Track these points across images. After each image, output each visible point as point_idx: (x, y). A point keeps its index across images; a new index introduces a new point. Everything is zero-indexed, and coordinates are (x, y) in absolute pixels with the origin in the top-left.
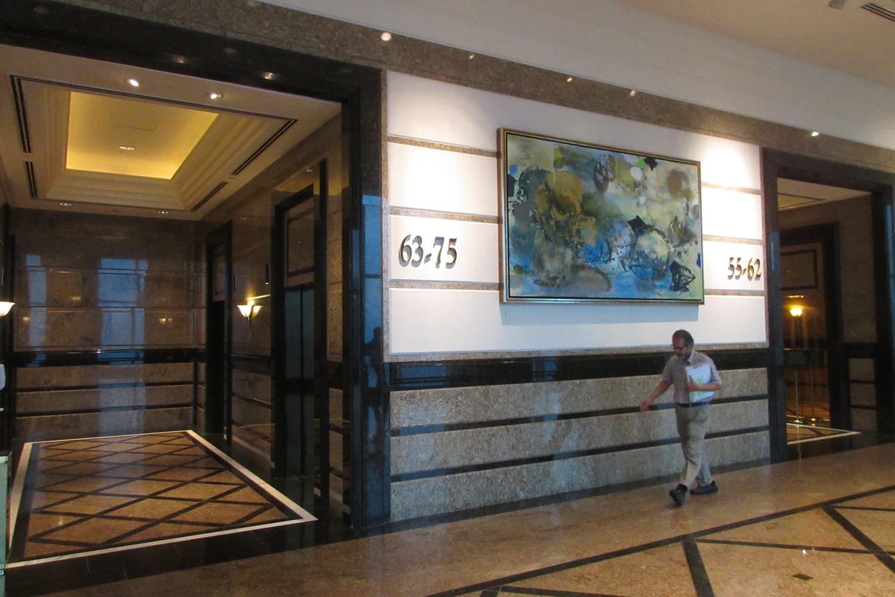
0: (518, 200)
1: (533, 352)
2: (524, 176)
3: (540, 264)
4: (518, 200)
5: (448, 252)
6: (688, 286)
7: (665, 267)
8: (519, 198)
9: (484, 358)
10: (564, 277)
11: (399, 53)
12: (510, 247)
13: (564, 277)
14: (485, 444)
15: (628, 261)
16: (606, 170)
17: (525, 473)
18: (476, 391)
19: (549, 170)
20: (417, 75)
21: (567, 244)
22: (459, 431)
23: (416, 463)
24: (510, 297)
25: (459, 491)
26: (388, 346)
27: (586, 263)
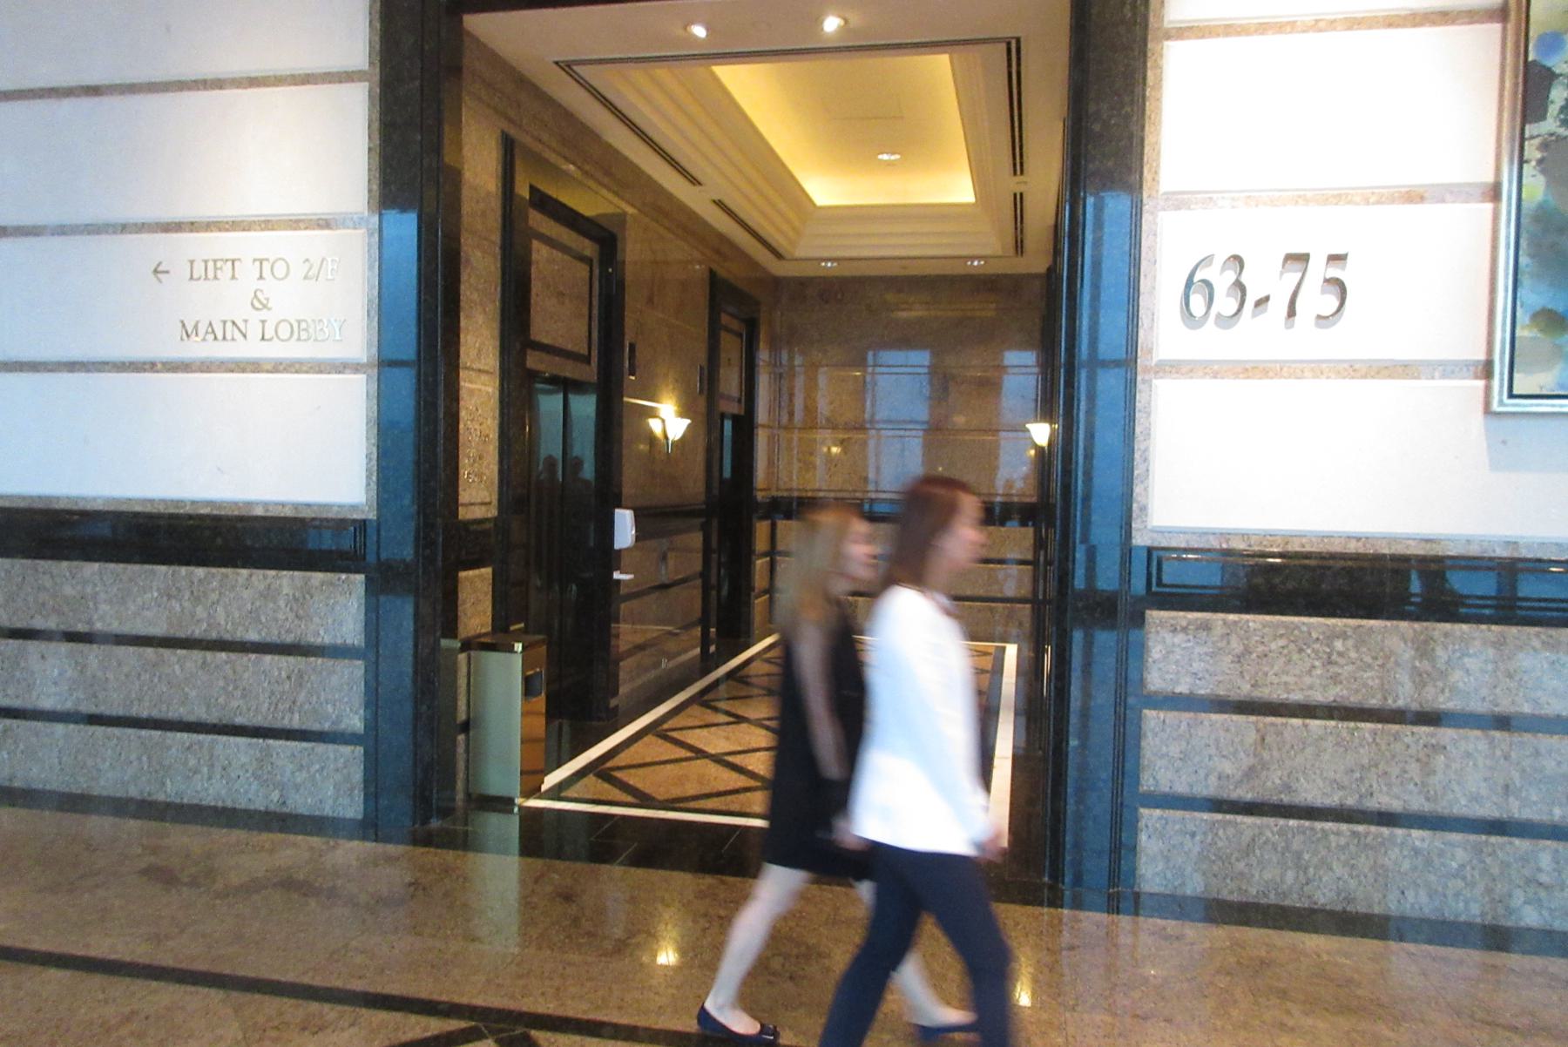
5: (1229, 289)
12: (1523, 260)
17: (1545, 860)
22: (1333, 723)
23: (1207, 776)
24: (1511, 396)
25: (1325, 864)
26: (1144, 509)
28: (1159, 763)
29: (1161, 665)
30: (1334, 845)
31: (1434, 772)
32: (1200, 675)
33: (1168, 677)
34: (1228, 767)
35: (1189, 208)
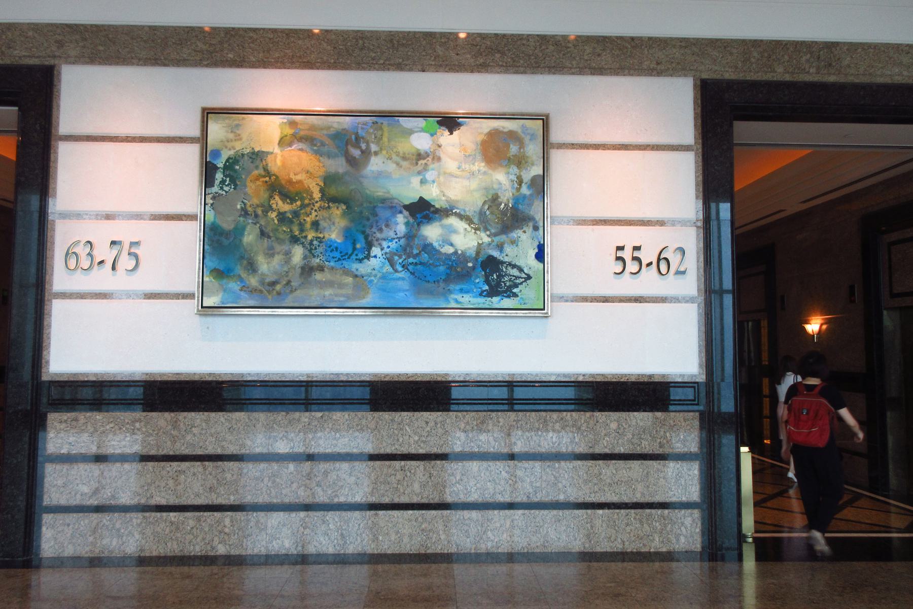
0: (220, 192)
1: (249, 374)
2: (231, 161)
3: (252, 267)
4: (220, 192)
6: (515, 290)
7: (470, 265)
8: (222, 188)
9: (175, 379)
10: (289, 282)
11: (78, 43)
13: (289, 282)
14: (171, 482)
15: (400, 257)
16: (368, 143)
17: (227, 521)
18: (162, 419)
19: (271, 150)
20: (100, 64)
21: (295, 240)
23: (76, 494)
24: (202, 307)
26: (48, 362)
27: (327, 263)
28: (53, 489)
29: (54, 440)
30: (135, 524)
31: (180, 484)
32: (73, 444)
33: (58, 445)
34: (85, 489)
35: (70, 219)
